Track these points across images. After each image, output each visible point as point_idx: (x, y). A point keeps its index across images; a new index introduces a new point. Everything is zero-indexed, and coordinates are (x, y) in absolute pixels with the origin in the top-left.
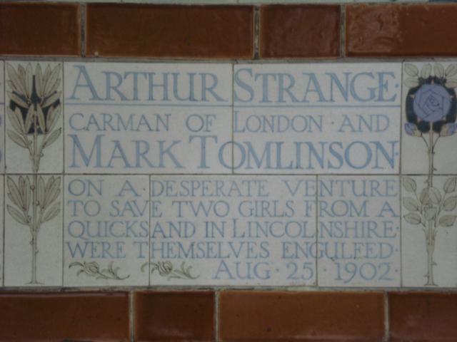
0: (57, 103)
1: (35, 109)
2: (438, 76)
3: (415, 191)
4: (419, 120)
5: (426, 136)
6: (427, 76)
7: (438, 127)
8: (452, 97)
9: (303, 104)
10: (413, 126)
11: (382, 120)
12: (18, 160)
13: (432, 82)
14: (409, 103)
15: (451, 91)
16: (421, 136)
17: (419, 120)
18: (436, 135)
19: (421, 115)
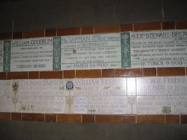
0: (18, 86)
1: (15, 87)
7: (71, 89)
12: (13, 94)
14: (66, 85)
15: (72, 83)
19: (68, 87)
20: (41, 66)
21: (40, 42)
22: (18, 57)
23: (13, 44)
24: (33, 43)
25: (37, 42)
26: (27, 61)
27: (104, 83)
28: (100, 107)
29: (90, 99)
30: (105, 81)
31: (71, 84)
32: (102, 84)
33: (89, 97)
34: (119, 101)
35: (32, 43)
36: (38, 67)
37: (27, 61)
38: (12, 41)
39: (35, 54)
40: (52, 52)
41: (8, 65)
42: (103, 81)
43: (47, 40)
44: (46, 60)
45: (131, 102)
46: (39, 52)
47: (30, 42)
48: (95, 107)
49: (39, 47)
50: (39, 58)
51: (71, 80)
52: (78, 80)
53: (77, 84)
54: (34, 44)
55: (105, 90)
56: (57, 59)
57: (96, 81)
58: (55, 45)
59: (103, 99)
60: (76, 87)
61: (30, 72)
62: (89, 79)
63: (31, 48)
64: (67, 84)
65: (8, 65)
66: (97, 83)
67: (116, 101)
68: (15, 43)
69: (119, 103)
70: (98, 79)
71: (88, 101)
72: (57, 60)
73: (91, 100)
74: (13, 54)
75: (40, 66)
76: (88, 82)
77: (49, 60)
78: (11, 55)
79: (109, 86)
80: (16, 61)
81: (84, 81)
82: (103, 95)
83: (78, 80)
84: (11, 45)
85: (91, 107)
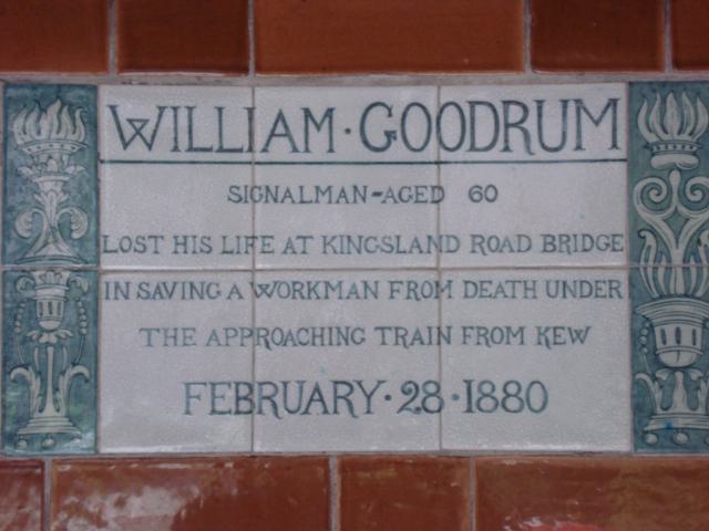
20: (487, 403)
21: (467, 126)
22: (199, 291)
23: (129, 131)
24: (390, 135)
25: (434, 124)
26: (317, 336)
35: (378, 139)
36: (455, 409)
37: (317, 336)
38: (108, 95)
39: (406, 261)
40: (623, 242)
41: (64, 382)
43: (552, 112)
44: (550, 337)
46: (467, 242)
47: (347, 117)
49: (458, 179)
50: (458, 311)
54: (397, 151)
56: (686, 331)
58: (656, 173)
61: (353, 465)
63: (360, 194)
65: (64, 382)
68: (152, 116)
72: (686, 339)
74: (138, 245)
75: (476, 397)
77: (579, 336)
78: (108, 263)
80: (177, 337)
84: (109, 145)
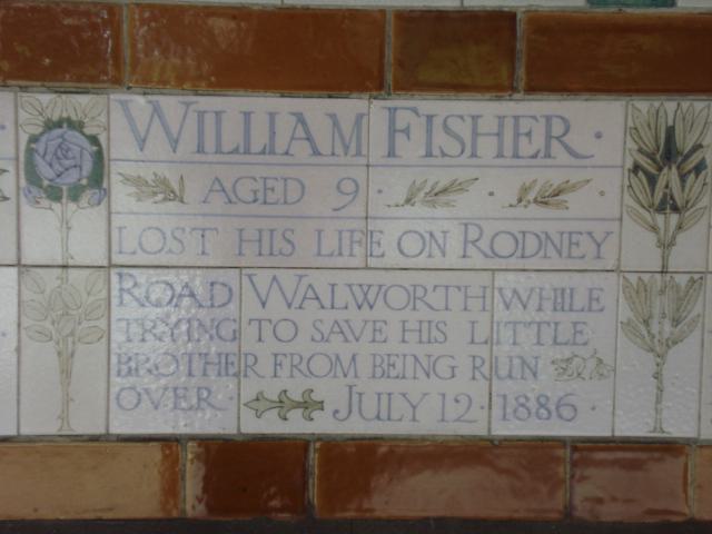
2: (74, 118)
3: (42, 293)
4: (46, 183)
5: (56, 206)
6: (55, 118)
7: (75, 196)
8: (95, 148)
9: (286, 159)
10: (34, 190)
11: (292, 185)
13: (65, 125)
14: (30, 152)
15: (94, 140)
16: (50, 208)
17: (46, 183)
18: (72, 206)
19: (46, 172)
27: (411, 149)
28: (364, 367)
29: (275, 300)
30: (418, 133)
31: (86, 143)
32: (391, 153)
33: (262, 279)
34: (547, 315)
42: (400, 125)
45: (655, 328)
48: (320, 365)
51: (80, 104)
52: (157, 110)
53: (142, 143)
55: (419, 210)
57: (336, 124)
59: (398, 298)
60: (127, 179)
62: (262, 104)
64: (40, 147)
66: (346, 148)
67: (517, 313)
69: (547, 336)
70: (348, 107)
71: (252, 308)
73: (276, 307)
76: (259, 139)
79: (462, 175)
81: (210, 120)
82: (393, 258)
83: (157, 110)
85: (284, 372)
